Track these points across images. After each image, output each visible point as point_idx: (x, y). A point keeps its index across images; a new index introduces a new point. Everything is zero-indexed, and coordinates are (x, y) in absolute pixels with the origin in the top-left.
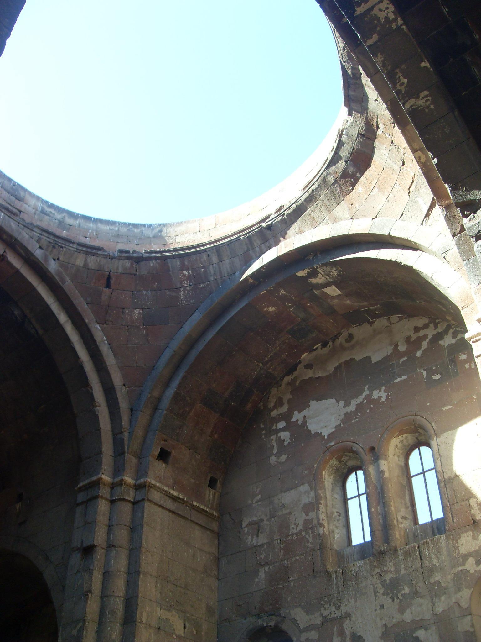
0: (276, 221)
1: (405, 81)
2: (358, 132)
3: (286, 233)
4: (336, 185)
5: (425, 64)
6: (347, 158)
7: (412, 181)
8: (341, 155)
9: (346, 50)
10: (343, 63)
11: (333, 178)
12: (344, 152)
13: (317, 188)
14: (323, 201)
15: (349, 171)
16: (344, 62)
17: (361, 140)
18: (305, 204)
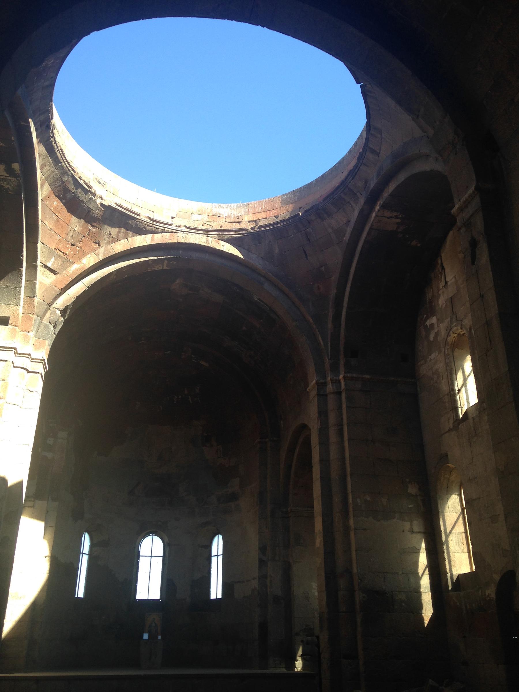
0: (51, 132)
1: (125, 270)
2: (92, 209)
3: (41, 143)
4: (60, 182)
5: (126, 276)
6: (77, 195)
7: (63, 252)
8: (79, 189)
9: (144, 229)
10: (136, 220)
11: (65, 180)
12: (80, 193)
13: (62, 166)
14: (54, 172)
15: (68, 194)
16: (137, 222)
17: (86, 210)
18: (55, 156)
